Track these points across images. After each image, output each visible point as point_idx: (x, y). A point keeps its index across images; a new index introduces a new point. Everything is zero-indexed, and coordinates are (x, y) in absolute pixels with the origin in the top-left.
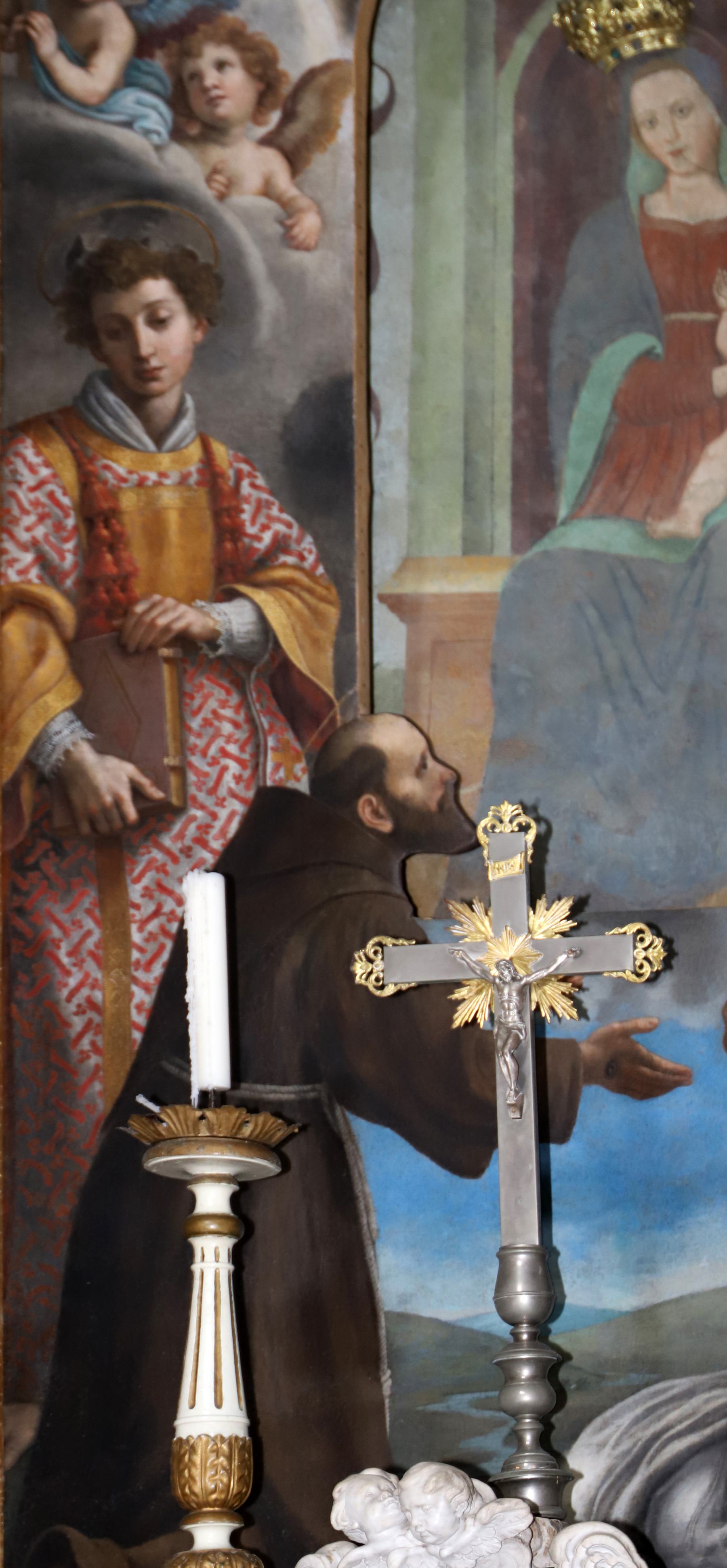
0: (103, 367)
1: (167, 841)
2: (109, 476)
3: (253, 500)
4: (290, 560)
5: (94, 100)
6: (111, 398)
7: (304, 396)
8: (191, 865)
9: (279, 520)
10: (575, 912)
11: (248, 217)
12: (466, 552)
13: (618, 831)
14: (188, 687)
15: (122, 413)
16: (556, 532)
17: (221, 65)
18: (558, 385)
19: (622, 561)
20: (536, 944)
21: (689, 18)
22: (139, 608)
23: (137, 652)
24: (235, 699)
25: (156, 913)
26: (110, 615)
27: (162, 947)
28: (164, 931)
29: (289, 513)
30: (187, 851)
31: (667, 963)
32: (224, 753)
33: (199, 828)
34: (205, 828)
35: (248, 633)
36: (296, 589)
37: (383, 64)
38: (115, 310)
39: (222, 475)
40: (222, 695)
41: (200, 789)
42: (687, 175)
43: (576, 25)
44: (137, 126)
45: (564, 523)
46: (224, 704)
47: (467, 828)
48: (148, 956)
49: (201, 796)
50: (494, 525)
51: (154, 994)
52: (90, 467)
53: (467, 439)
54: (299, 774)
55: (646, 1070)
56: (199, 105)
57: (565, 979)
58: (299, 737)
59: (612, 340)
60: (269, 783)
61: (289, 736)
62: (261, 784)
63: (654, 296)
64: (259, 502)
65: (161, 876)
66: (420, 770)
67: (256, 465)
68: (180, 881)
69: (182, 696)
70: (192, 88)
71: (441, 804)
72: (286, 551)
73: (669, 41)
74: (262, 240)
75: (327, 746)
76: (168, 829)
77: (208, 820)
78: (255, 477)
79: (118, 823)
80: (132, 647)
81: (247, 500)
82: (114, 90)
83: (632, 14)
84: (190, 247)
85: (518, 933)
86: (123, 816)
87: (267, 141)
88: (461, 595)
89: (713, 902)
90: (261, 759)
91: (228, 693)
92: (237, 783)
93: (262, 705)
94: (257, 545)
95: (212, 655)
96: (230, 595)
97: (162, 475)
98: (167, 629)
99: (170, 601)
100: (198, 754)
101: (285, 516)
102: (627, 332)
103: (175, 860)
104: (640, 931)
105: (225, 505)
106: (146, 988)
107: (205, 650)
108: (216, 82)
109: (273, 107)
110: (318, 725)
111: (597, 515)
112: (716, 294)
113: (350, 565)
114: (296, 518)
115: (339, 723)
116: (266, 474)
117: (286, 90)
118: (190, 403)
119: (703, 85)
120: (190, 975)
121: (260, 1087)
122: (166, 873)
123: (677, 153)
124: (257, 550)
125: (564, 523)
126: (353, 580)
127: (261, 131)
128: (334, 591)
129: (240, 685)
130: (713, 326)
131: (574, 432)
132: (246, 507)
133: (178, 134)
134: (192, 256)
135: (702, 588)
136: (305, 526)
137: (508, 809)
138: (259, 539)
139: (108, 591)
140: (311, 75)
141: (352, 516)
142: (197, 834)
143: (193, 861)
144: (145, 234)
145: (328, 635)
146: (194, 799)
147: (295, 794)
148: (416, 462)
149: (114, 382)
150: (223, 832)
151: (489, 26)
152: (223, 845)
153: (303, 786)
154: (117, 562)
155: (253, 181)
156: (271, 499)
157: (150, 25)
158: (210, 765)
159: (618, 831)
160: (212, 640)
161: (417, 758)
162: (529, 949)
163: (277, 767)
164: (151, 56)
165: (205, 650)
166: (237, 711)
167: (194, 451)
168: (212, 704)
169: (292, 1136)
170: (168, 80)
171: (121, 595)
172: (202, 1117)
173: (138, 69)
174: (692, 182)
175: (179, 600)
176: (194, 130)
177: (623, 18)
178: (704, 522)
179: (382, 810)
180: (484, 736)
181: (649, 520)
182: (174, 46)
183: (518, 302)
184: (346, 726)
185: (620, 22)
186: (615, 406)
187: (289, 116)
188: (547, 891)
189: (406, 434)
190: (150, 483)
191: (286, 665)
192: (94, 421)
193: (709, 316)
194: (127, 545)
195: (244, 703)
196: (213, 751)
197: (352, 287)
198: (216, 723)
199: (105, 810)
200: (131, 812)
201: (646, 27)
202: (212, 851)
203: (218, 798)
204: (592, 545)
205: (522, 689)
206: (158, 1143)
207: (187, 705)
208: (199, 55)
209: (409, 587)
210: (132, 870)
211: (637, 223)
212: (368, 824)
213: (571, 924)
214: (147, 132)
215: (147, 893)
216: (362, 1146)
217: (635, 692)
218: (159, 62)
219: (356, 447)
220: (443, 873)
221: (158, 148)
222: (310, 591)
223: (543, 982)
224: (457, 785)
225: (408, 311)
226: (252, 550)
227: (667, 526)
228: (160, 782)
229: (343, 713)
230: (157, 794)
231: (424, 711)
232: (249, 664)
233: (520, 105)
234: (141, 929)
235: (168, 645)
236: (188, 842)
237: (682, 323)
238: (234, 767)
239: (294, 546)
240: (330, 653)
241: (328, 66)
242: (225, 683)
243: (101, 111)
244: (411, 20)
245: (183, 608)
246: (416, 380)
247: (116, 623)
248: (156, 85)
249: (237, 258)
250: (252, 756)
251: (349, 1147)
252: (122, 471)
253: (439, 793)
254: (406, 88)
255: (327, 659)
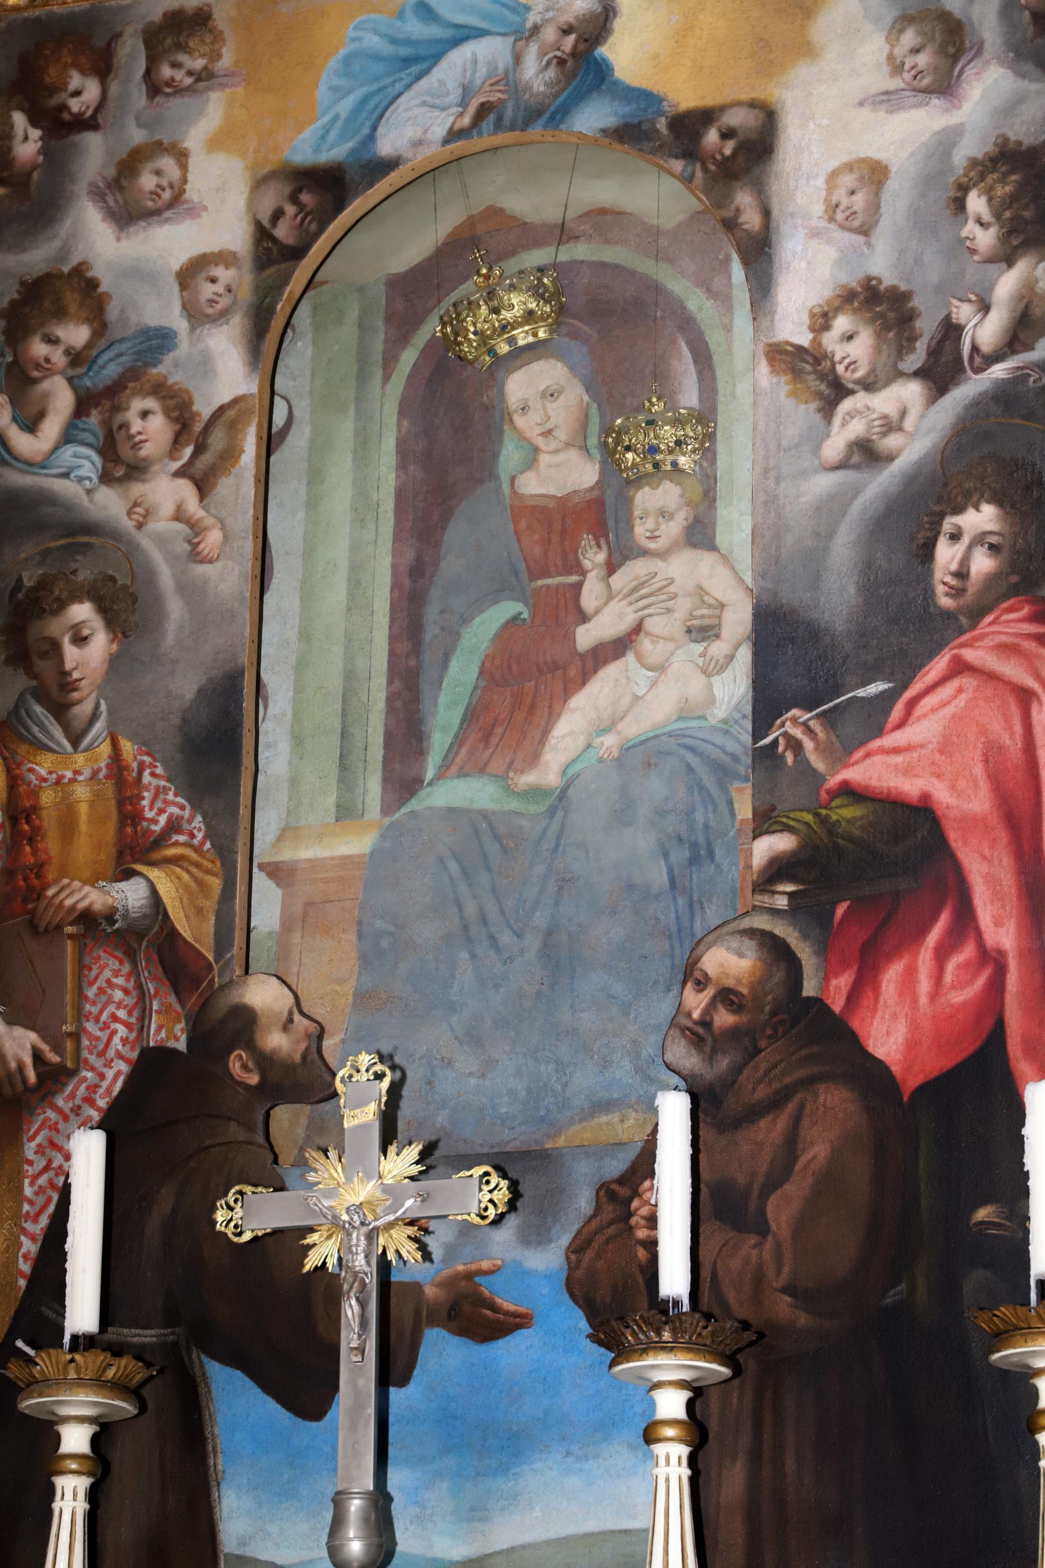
0: (34, 683)
1: (60, 1102)
2: (33, 777)
3: (152, 787)
4: (182, 838)
5: (39, 459)
6: (38, 709)
7: (200, 690)
8: (79, 1123)
9: (174, 803)
10: (424, 1156)
11: (161, 540)
12: (337, 821)
13: (471, 1074)
14: (87, 960)
15: (46, 722)
16: (422, 794)
17: (145, 414)
18: (430, 657)
19: (484, 815)
20: (387, 1189)
21: (561, 310)
22: (50, 892)
23: (46, 930)
24: (126, 968)
25: (46, 1168)
26: (25, 901)
27: (49, 1199)
28: (52, 1184)
29: (183, 797)
30: (77, 1110)
31: (512, 1205)
32: (114, 1018)
33: (88, 1088)
34: (93, 1088)
35: (141, 907)
36: (186, 864)
37: (283, 393)
38: (47, 634)
39: (127, 768)
40: (116, 965)
41: (91, 1053)
42: (556, 451)
43: (457, 335)
44: (72, 476)
45: (430, 784)
46: (116, 973)
47: (327, 1077)
48: (37, 1208)
49: (92, 1059)
50: (365, 791)
51: (39, 1243)
52: (18, 772)
53: (344, 714)
54: (179, 1034)
55: (488, 1312)
56: (125, 451)
57: (412, 1223)
58: (181, 1001)
59: (482, 611)
60: (151, 1044)
61: (172, 999)
62: (145, 1045)
63: (522, 566)
64: (157, 788)
65: (54, 1133)
66: (288, 1024)
67: (157, 756)
68: (68, 1137)
69: (82, 967)
70: (120, 437)
71: (304, 1057)
72: (179, 831)
73: (542, 334)
74: (172, 558)
75: (204, 1006)
76: (62, 1090)
77: (97, 1080)
78: (156, 767)
79: (20, 1087)
80: (41, 929)
81: (147, 788)
82: (55, 449)
83: (507, 315)
84: (110, 572)
85: (369, 1178)
86: (24, 1080)
87: (179, 474)
88: (333, 858)
89: (561, 1142)
90: (147, 1022)
91: (121, 963)
92: (124, 1045)
93: (149, 972)
94: (153, 827)
95: (109, 931)
96: (128, 874)
97: (76, 772)
98: (73, 908)
99: (76, 884)
100: (92, 1020)
101: (179, 799)
102: (496, 602)
103: (66, 1118)
104: (486, 1174)
105: (129, 794)
106: (33, 1238)
107: (104, 925)
108: (140, 429)
109: (188, 444)
110: (198, 989)
111: (462, 774)
112: (581, 557)
113: (233, 839)
114: (189, 801)
115: (217, 985)
116: (165, 764)
117: (198, 427)
118: (103, 707)
119: (572, 369)
120: (70, 1226)
121: (125, 1331)
122: (58, 1131)
123: (547, 433)
124: (154, 831)
125: (430, 784)
126: (237, 853)
127: (176, 465)
128: (218, 864)
129: (131, 955)
130: (578, 587)
131: (443, 699)
132: (146, 794)
133: (106, 478)
134: (113, 579)
135: (559, 837)
136: (195, 808)
137: (365, 1059)
138: (155, 821)
139: (25, 879)
140: (222, 410)
141: (238, 793)
142: (87, 1095)
143: (82, 1119)
144: (74, 566)
145: (210, 905)
146: (86, 1061)
147: (174, 1052)
148: (298, 740)
149: (41, 695)
150: (109, 1090)
151: (378, 345)
152: (108, 1103)
153: (181, 1045)
154: (34, 853)
155: (167, 508)
156: (168, 785)
157: (88, 389)
158: (101, 1029)
159: (471, 1074)
160: (110, 917)
161: (285, 1014)
162: (379, 1194)
163: (159, 1029)
164: (88, 415)
165: (104, 925)
166: (128, 980)
167: (105, 749)
168: (107, 974)
169: (151, 1378)
170: (101, 435)
171: (36, 881)
172: (72, 1361)
173: (76, 428)
174: (560, 457)
175: (85, 883)
176: (120, 472)
177: (500, 321)
178: (564, 772)
179: (250, 1064)
180: (349, 988)
181: (511, 774)
182: (107, 404)
183: (395, 586)
184: (222, 987)
185: (497, 324)
186: (482, 672)
187: (199, 450)
188: (400, 1136)
189: (290, 716)
190: (66, 781)
191: (174, 933)
192: (23, 731)
193: (574, 579)
194: (43, 837)
195: (135, 972)
196: (104, 1017)
197: (248, 589)
198: (109, 991)
199: (9, 1074)
200: (32, 1076)
201: (521, 325)
202: (98, 1109)
203: (106, 1060)
204: (457, 803)
205: (385, 943)
206: (33, 1385)
207: (86, 976)
208: (128, 408)
209: (286, 855)
210: (29, 1130)
211: (508, 501)
212: (238, 1078)
213: (420, 1168)
214: (81, 479)
215: (40, 1150)
216: (213, 1387)
217: (492, 938)
218: (94, 419)
219: (245, 731)
220: (304, 1121)
221: (89, 492)
222: (198, 865)
223: (390, 1225)
224: (320, 1037)
225: (297, 605)
226: (149, 832)
227: (529, 779)
228: (57, 1049)
229: (220, 977)
230: (55, 1058)
231: (295, 969)
232: (140, 936)
233: (404, 409)
234: (32, 1184)
235: (70, 924)
236: (78, 1101)
237: (548, 586)
238: (122, 1030)
239: (185, 826)
240: (212, 921)
241: (235, 401)
242: (119, 954)
243: (44, 467)
244: (309, 352)
245: (87, 889)
246: (300, 667)
247: (30, 906)
248: (91, 439)
249: (150, 577)
250: (137, 1019)
251: (202, 1389)
252: (43, 772)
253: (303, 1046)
254: (303, 409)
255: (209, 926)
